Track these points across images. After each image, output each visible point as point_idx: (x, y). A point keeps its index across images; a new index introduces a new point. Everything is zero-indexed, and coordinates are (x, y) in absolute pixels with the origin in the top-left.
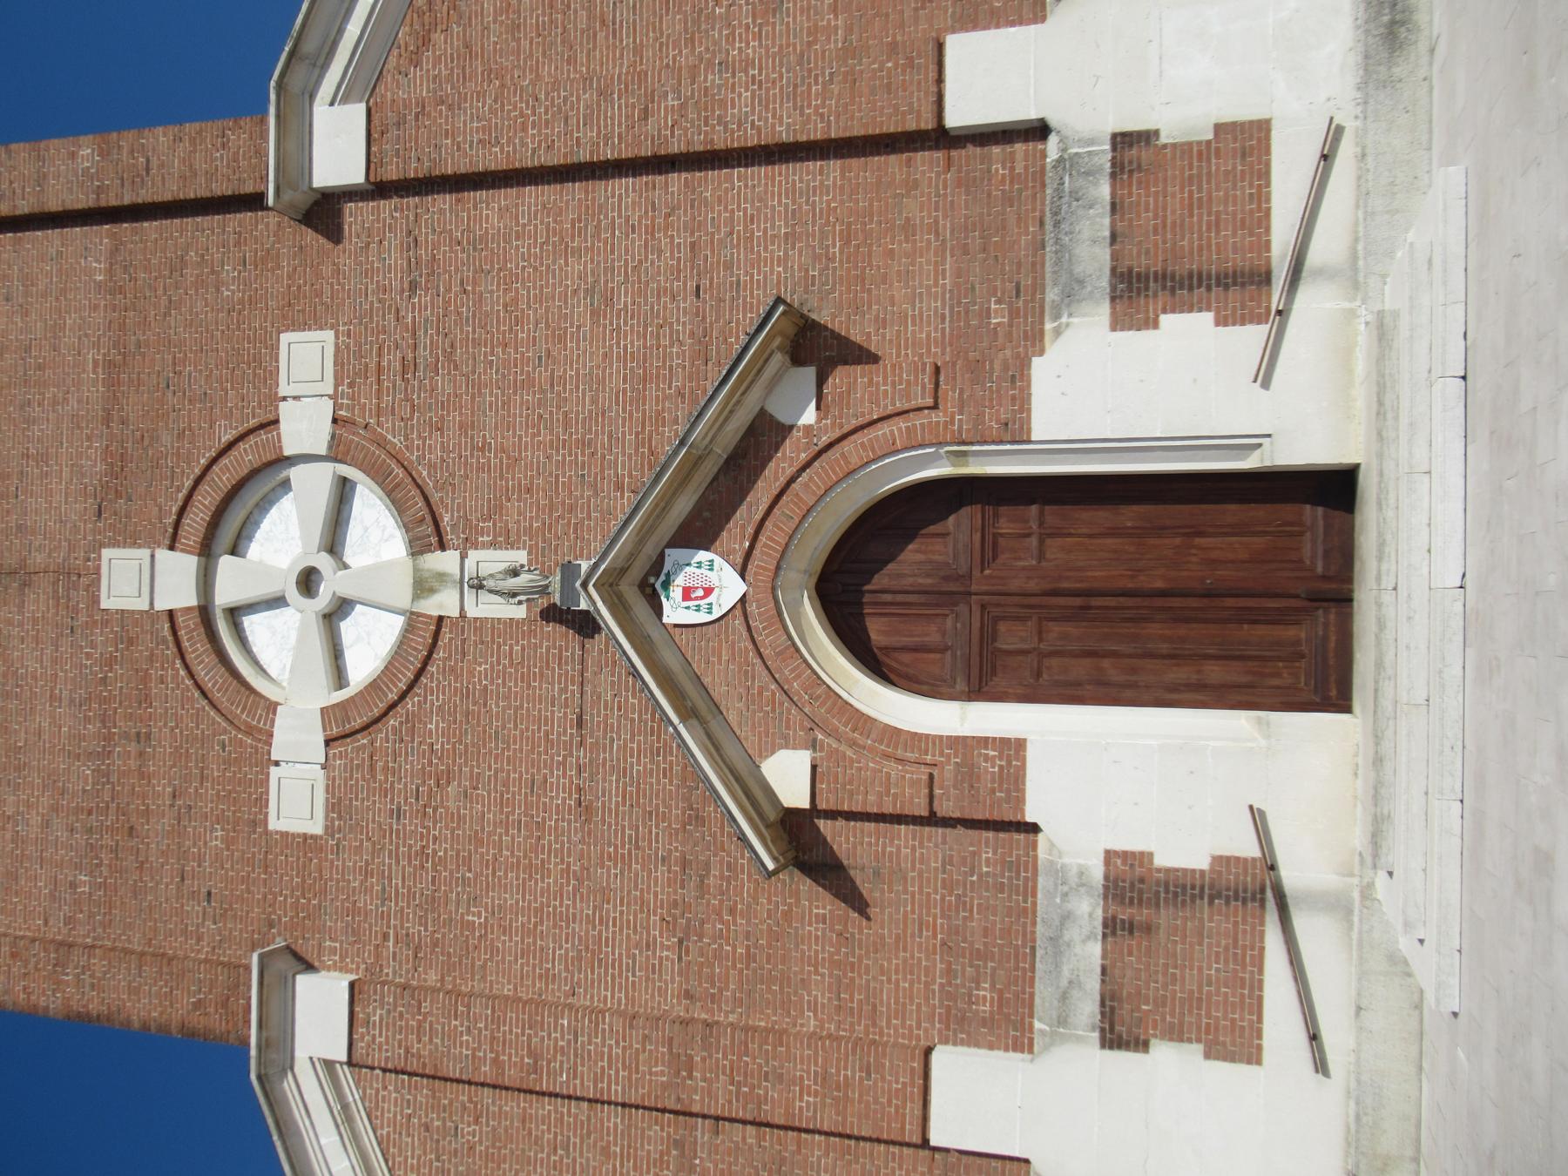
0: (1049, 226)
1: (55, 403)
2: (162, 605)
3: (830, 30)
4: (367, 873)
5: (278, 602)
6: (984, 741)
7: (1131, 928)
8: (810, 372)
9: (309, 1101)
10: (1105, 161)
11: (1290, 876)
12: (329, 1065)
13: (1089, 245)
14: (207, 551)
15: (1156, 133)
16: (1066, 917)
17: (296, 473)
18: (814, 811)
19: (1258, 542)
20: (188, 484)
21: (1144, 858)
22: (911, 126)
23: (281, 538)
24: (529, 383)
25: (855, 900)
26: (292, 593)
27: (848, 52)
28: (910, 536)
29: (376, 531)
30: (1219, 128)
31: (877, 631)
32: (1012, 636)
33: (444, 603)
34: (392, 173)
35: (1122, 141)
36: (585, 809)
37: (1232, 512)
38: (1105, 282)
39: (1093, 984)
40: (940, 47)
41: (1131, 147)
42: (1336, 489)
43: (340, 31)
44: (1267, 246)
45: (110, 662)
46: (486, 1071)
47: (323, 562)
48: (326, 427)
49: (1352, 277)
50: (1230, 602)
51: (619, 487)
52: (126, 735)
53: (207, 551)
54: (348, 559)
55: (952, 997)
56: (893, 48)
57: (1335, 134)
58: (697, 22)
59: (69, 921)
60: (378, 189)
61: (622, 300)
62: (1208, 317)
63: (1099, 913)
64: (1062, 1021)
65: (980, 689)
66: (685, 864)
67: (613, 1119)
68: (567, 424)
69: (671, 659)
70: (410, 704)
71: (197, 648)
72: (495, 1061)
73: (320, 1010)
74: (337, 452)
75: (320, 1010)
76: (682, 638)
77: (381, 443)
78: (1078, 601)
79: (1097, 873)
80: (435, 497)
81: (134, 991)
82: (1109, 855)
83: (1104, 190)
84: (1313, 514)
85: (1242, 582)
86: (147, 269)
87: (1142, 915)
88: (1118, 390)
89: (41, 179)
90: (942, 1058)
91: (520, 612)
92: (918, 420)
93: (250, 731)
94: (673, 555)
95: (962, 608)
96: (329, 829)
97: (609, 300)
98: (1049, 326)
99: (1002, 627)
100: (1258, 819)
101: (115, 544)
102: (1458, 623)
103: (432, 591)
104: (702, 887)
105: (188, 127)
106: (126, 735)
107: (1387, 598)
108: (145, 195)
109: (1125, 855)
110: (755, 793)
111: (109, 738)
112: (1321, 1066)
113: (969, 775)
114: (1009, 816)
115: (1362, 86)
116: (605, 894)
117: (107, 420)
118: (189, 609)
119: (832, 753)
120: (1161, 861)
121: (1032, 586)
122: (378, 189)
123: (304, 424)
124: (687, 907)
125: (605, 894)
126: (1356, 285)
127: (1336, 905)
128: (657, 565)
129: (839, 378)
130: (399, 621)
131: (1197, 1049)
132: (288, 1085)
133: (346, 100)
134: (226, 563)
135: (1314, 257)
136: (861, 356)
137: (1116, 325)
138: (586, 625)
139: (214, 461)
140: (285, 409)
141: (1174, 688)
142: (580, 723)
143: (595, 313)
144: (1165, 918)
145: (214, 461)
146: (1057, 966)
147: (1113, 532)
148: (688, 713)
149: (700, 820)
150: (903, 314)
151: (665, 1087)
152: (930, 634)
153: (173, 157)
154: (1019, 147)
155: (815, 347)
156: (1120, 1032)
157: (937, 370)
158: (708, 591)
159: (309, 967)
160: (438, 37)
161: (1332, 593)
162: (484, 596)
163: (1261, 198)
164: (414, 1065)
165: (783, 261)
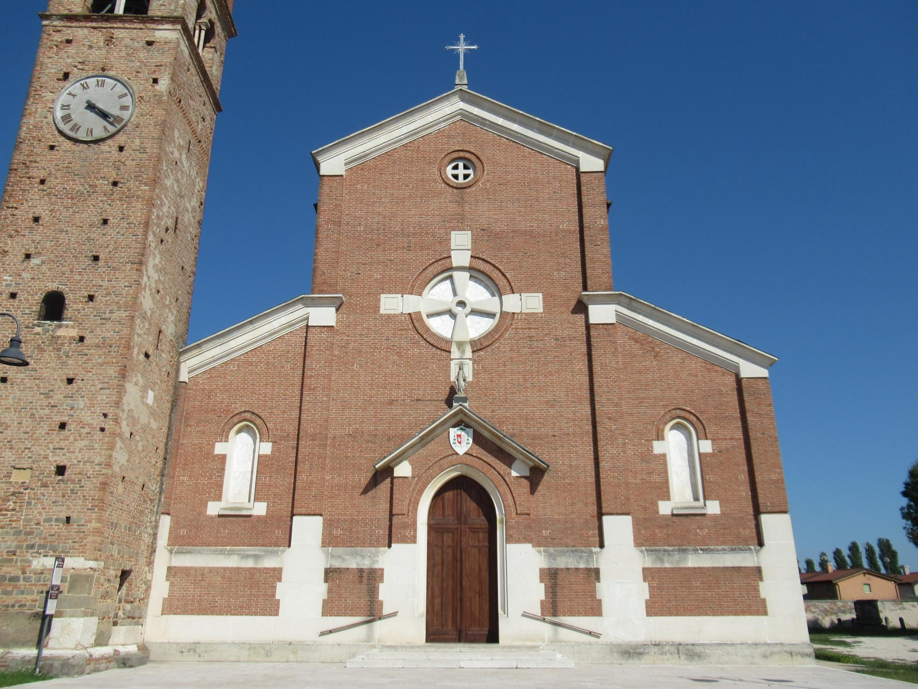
0: (573, 549)
1: (519, 212)
2: (453, 253)
3: (635, 478)
4: (368, 329)
5: (455, 294)
6: (415, 531)
7: (361, 577)
8: (527, 474)
9: (297, 313)
10: (591, 566)
11: (378, 624)
12: (307, 318)
13: (565, 561)
14: (470, 269)
15: (599, 582)
16: (363, 557)
17: (497, 298)
18: (393, 478)
19: (477, 614)
20: (493, 262)
21: (382, 580)
22: (604, 505)
23: (476, 293)
24: (525, 380)
25: (366, 491)
26: (458, 299)
27: (627, 484)
28: (478, 504)
29: (478, 327)
30: (600, 601)
31: (449, 495)
32: (448, 539)
33: (455, 353)
34: (593, 333)
35: (597, 572)
36: (391, 402)
37: (486, 606)
38: (554, 566)
39: (344, 566)
40: (628, 514)
41: (595, 574)
42: (492, 637)
43: (639, 313)
44: (564, 615)
45: (434, 236)
46: (308, 373)
47: (468, 309)
48: (511, 310)
49: (555, 641)
50: (459, 605)
51: (493, 411)
52: (409, 242)
53: (470, 269)
54: (470, 317)
55: (338, 521)
56: (628, 499)
58: (640, 434)
59: (348, 223)
60: (588, 326)
61: (552, 411)
62: (543, 598)
63: (365, 567)
64: (332, 556)
65: (431, 528)
66: (375, 436)
67: (295, 414)
68: (512, 393)
69: (438, 432)
70: (423, 342)
71: (438, 267)
72: (311, 376)
73: (324, 316)
74: (503, 314)
75: (323, 316)
76: (445, 434)
77: (507, 330)
78: (459, 558)
79: (377, 566)
80: (489, 349)
81: (327, 250)
82: (382, 570)
83: (582, 566)
84: (485, 631)
85: (464, 609)
86: (564, 244)
87: (365, 580)
88: (522, 569)
89: (594, 206)
90: (319, 519)
91: (453, 379)
92: (513, 509)
93: (413, 286)
94: (471, 431)
95: (456, 522)
96: (382, 316)
97: (552, 406)
98: (542, 549)
99: (451, 535)
100: (394, 614)
101: (473, 235)
102: (450, 666)
103: (459, 349)
104: (368, 442)
105: (609, 261)
106: (409, 242)
107: (458, 649)
108: (587, 245)
109: (382, 575)
110: (398, 460)
111: (409, 236)
112: (322, 634)
113: (405, 526)
114: (393, 539)
115: (611, 644)
116: (365, 410)
117: (513, 232)
118: (451, 263)
119: (411, 483)
120: (381, 585)
121: (463, 544)
122: (588, 326)
123: (513, 303)
124: (362, 437)
125: (365, 410)
126: (552, 642)
127: (369, 638)
128: (468, 426)
129: (526, 483)
130: (449, 337)
131: (326, 597)
132: (300, 306)
133: (617, 315)
134: (467, 275)
135: (562, 630)
136: (533, 490)
137: (541, 570)
138: (449, 403)
139: (500, 271)
140: (516, 296)
141: (433, 589)
142: (418, 400)
143: (547, 402)
144: (364, 587)
145: (500, 271)
146: (349, 555)
147: (480, 569)
148: (422, 438)
149: (389, 440)
150: (547, 502)
151: (307, 432)
152: (448, 512)
153: (600, 253)
154: (597, 539)
155: (536, 475)
156: (330, 574)
157: (529, 514)
158: (460, 443)
159: (337, 310)
160: (638, 346)
161: (462, 636)
162: (458, 370)
163: (579, 614)
164: (308, 349)
165: (563, 464)
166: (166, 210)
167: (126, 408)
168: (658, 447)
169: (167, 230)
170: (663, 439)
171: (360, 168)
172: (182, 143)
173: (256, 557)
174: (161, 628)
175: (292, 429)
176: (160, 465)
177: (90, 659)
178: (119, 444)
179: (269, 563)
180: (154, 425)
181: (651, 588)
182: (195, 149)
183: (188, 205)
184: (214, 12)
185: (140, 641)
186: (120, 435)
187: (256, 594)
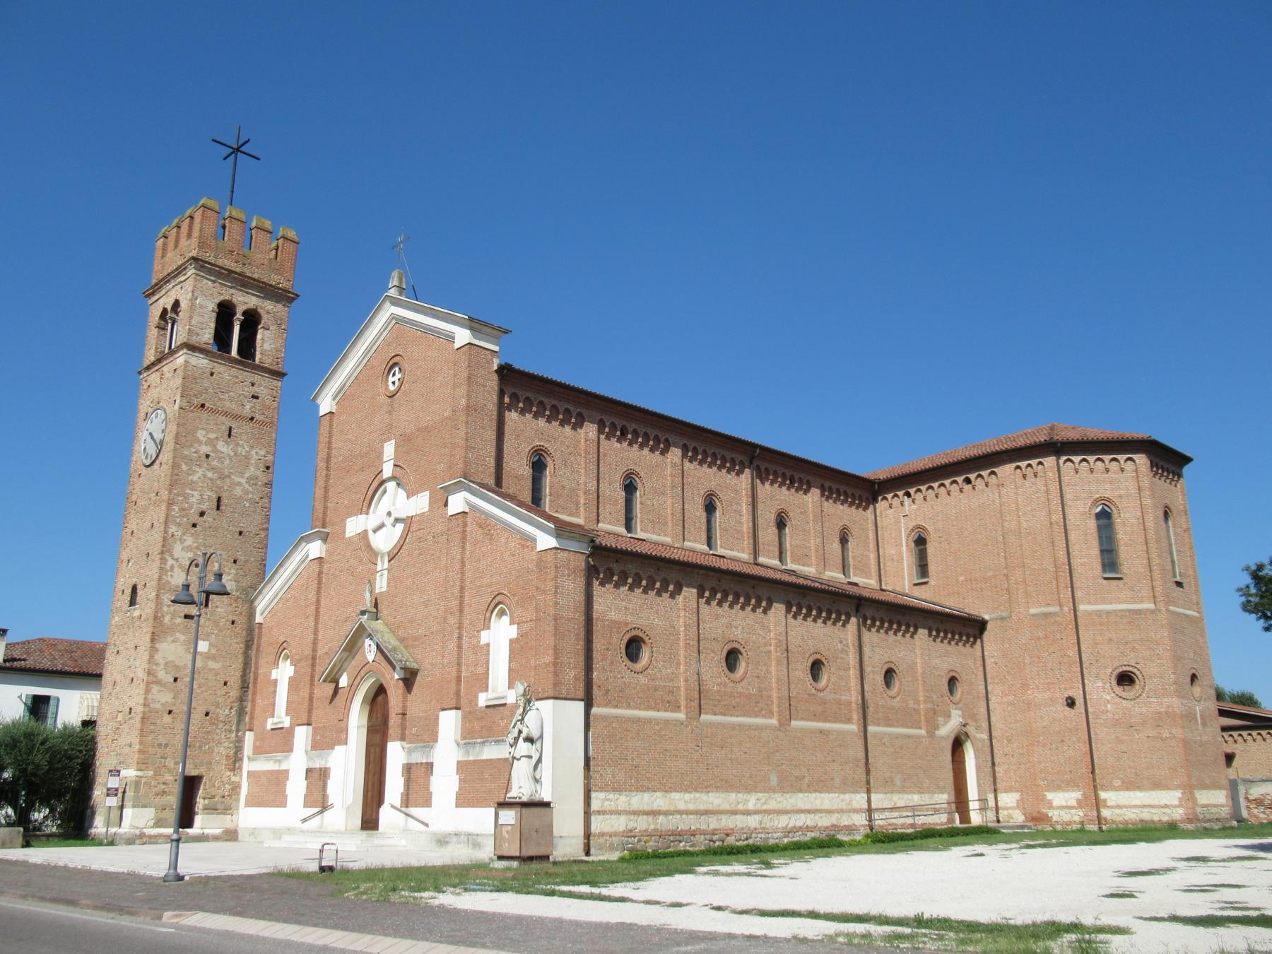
13: (418, 758)
41: (430, 766)
47: (392, 519)
49: (406, 830)
57: (427, 825)
73: (315, 549)
75: (315, 549)
129: (401, 683)
159: (325, 540)
166: (198, 498)
167: (162, 662)
168: (485, 637)
169: (202, 514)
170: (489, 628)
171: (343, 397)
172: (212, 436)
173: (280, 761)
174: (248, 817)
175: (308, 652)
176: (234, 693)
177: (142, 835)
178: (155, 688)
179: (284, 767)
180: (212, 664)
181: (460, 780)
182: (240, 429)
183: (237, 479)
184: (254, 299)
185: (230, 825)
186: (158, 683)
187: (271, 791)
